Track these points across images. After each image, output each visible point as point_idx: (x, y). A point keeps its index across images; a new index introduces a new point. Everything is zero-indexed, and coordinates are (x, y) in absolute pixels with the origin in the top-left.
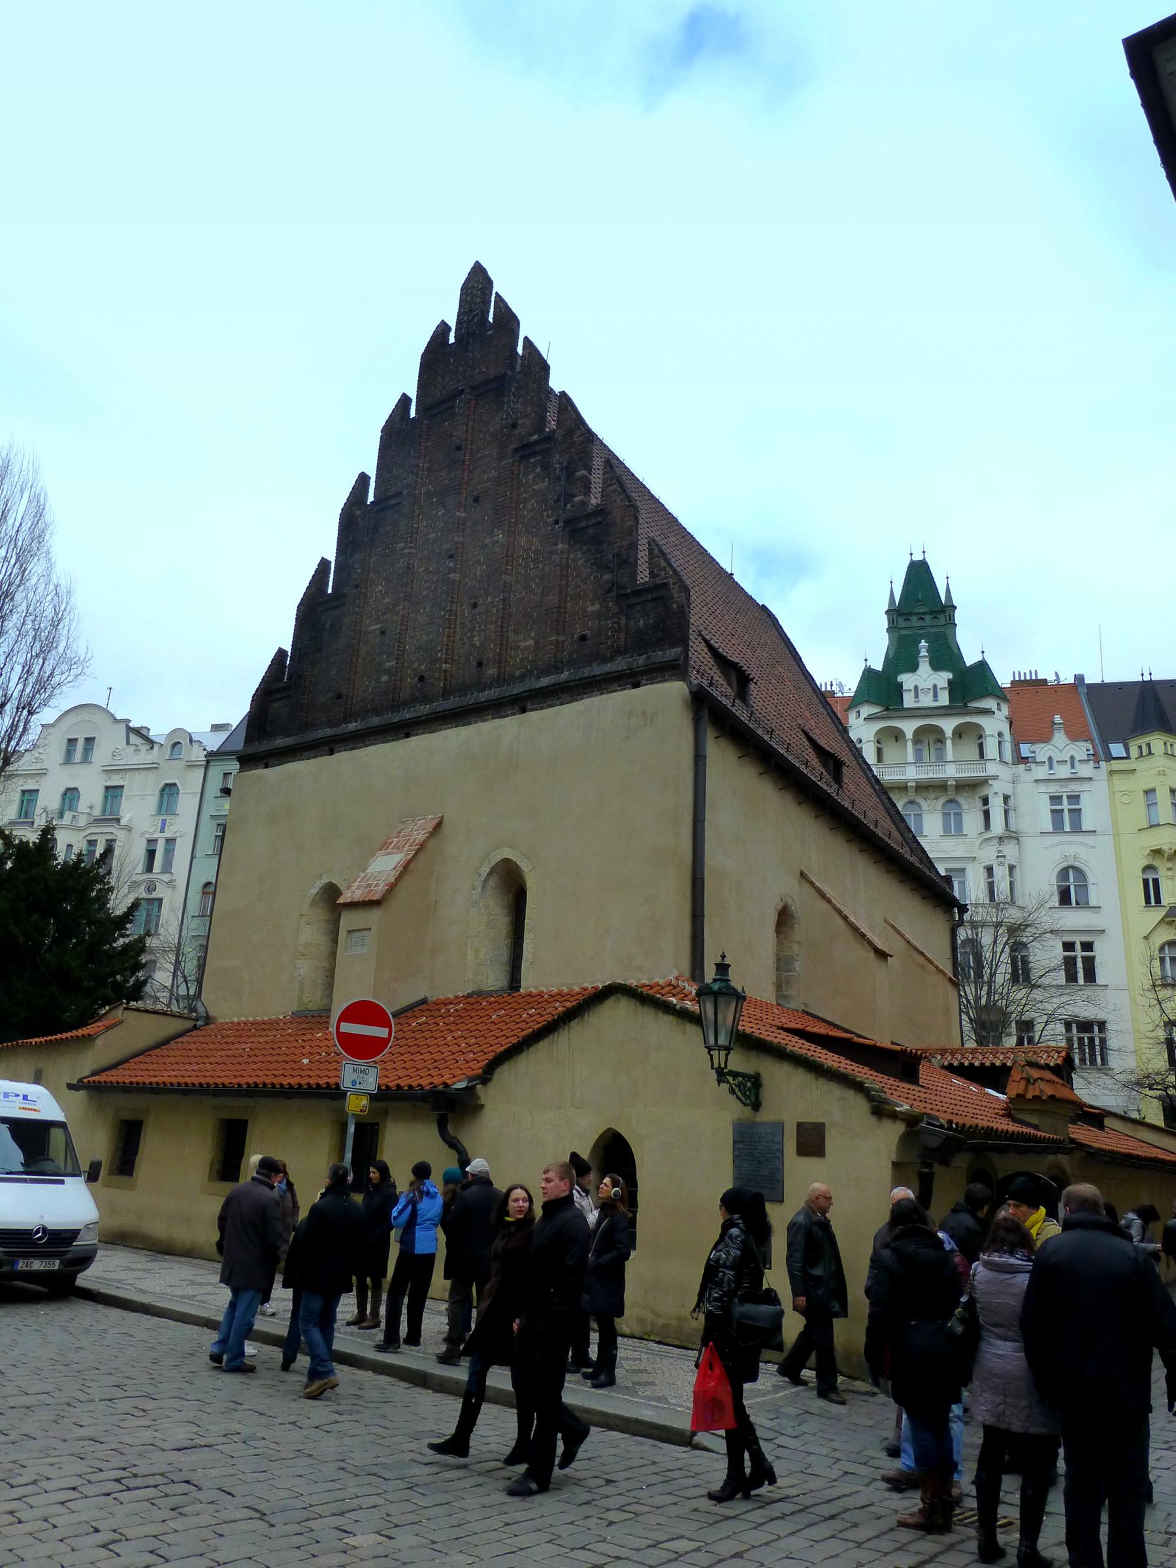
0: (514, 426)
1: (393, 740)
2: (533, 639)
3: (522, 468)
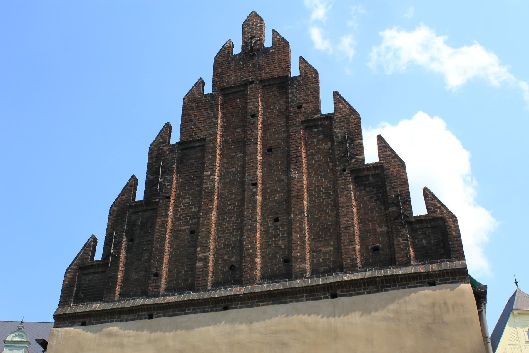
0: (300, 107)
1: (212, 311)
2: (332, 246)
3: (307, 134)
